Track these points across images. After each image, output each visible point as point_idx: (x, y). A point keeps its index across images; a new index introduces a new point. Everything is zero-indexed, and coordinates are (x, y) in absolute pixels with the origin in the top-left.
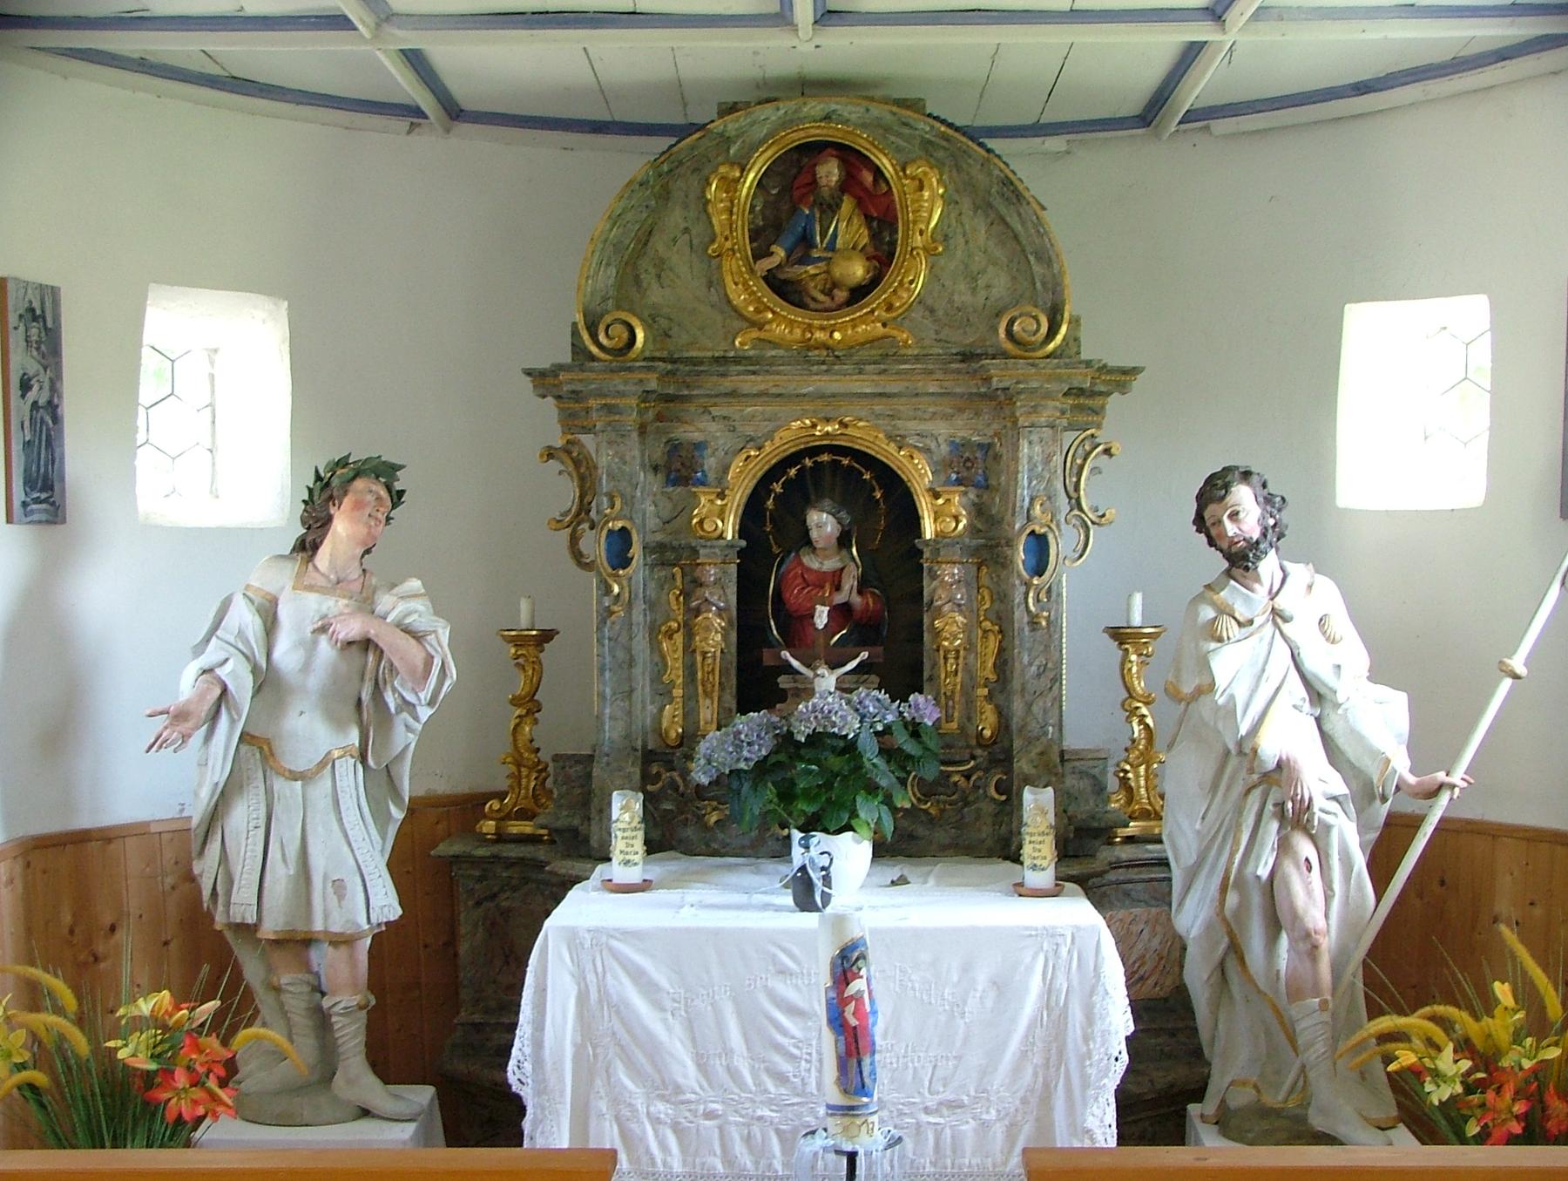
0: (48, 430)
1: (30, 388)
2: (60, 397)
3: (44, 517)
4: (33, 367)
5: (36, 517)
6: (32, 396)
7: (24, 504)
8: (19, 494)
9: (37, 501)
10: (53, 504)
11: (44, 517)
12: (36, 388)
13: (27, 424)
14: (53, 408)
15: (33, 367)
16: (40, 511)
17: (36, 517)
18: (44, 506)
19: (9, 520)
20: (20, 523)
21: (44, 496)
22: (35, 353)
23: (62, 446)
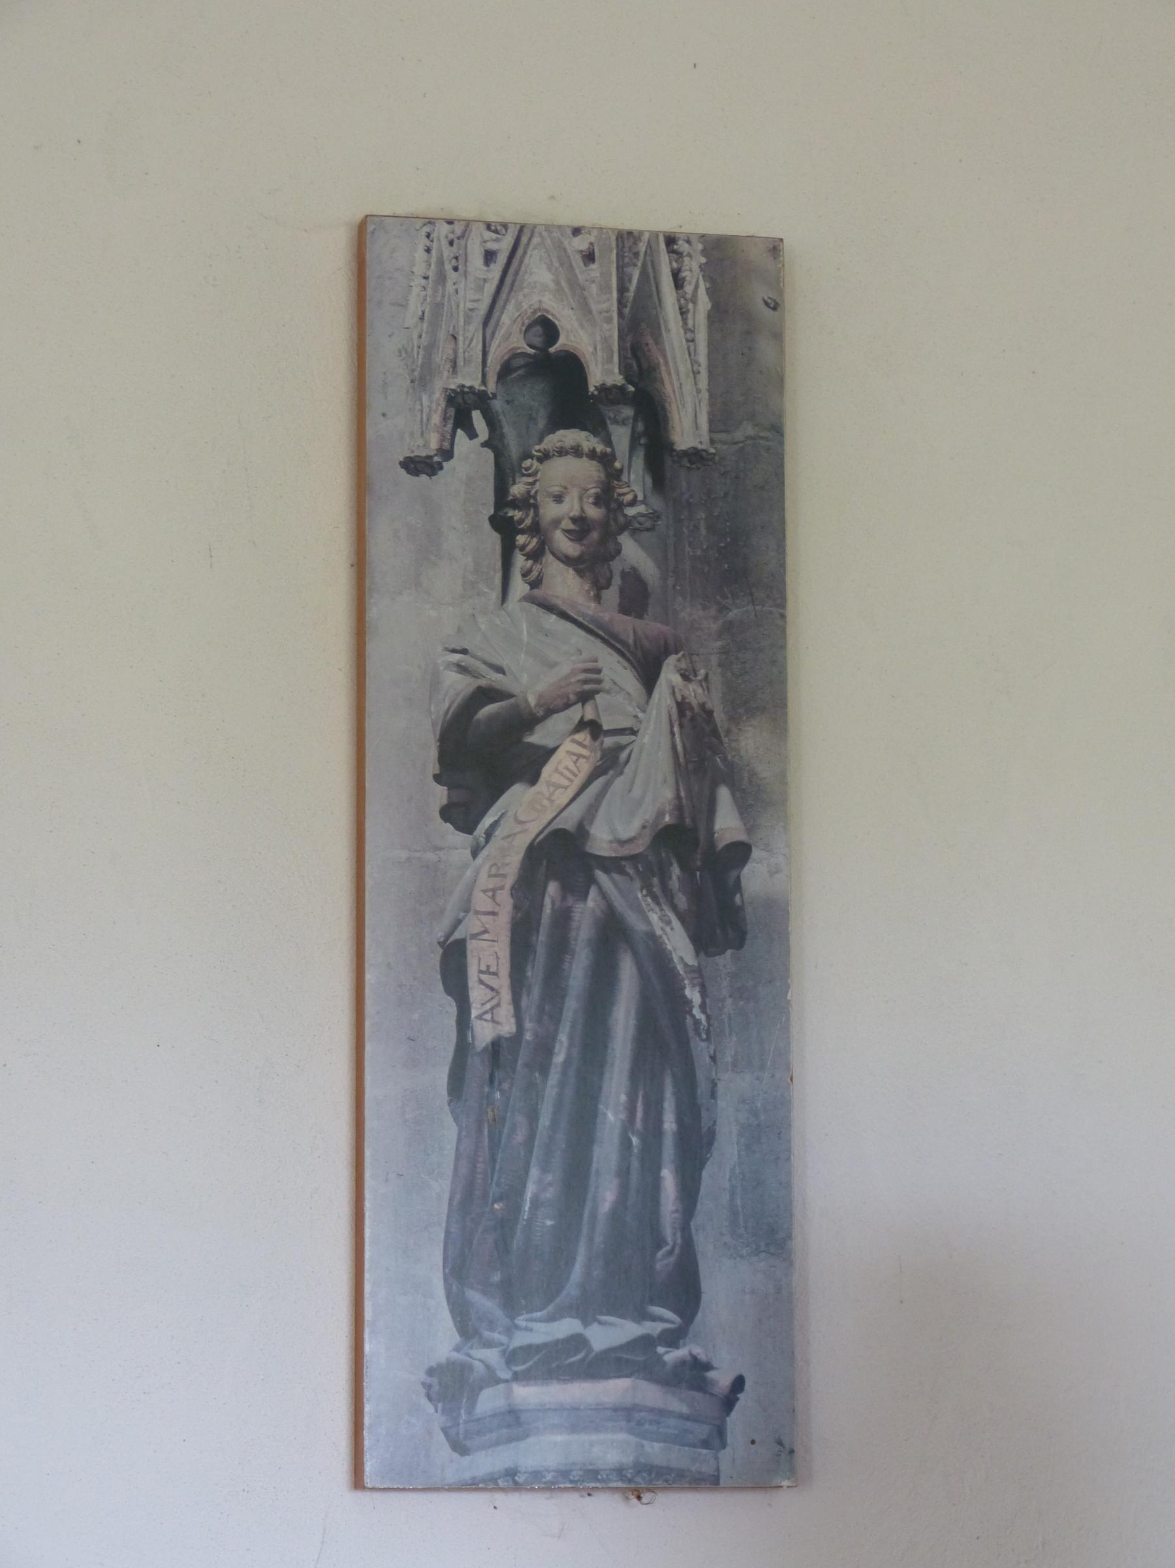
0: (657, 960)
1: (530, 766)
2: (761, 799)
3: (611, 1448)
4: (537, 654)
5: (546, 1450)
6: (525, 812)
7: (450, 1386)
8: (420, 1325)
9: (558, 1361)
10: (694, 1374)
11: (611, 1448)
12: (569, 761)
13: (489, 954)
14: (711, 877)
15: (537, 654)
16: (578, 1420)
17: (546, 1450)
18: (615, 1389)
19: (358, 1481)
20: (416, 1481)
21: (610, 1333)
22: (565, 584)
23: (773, 1060)
